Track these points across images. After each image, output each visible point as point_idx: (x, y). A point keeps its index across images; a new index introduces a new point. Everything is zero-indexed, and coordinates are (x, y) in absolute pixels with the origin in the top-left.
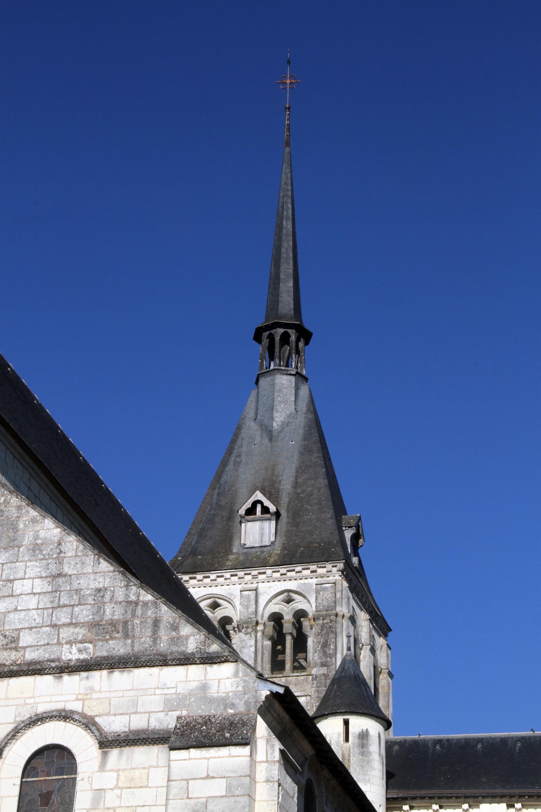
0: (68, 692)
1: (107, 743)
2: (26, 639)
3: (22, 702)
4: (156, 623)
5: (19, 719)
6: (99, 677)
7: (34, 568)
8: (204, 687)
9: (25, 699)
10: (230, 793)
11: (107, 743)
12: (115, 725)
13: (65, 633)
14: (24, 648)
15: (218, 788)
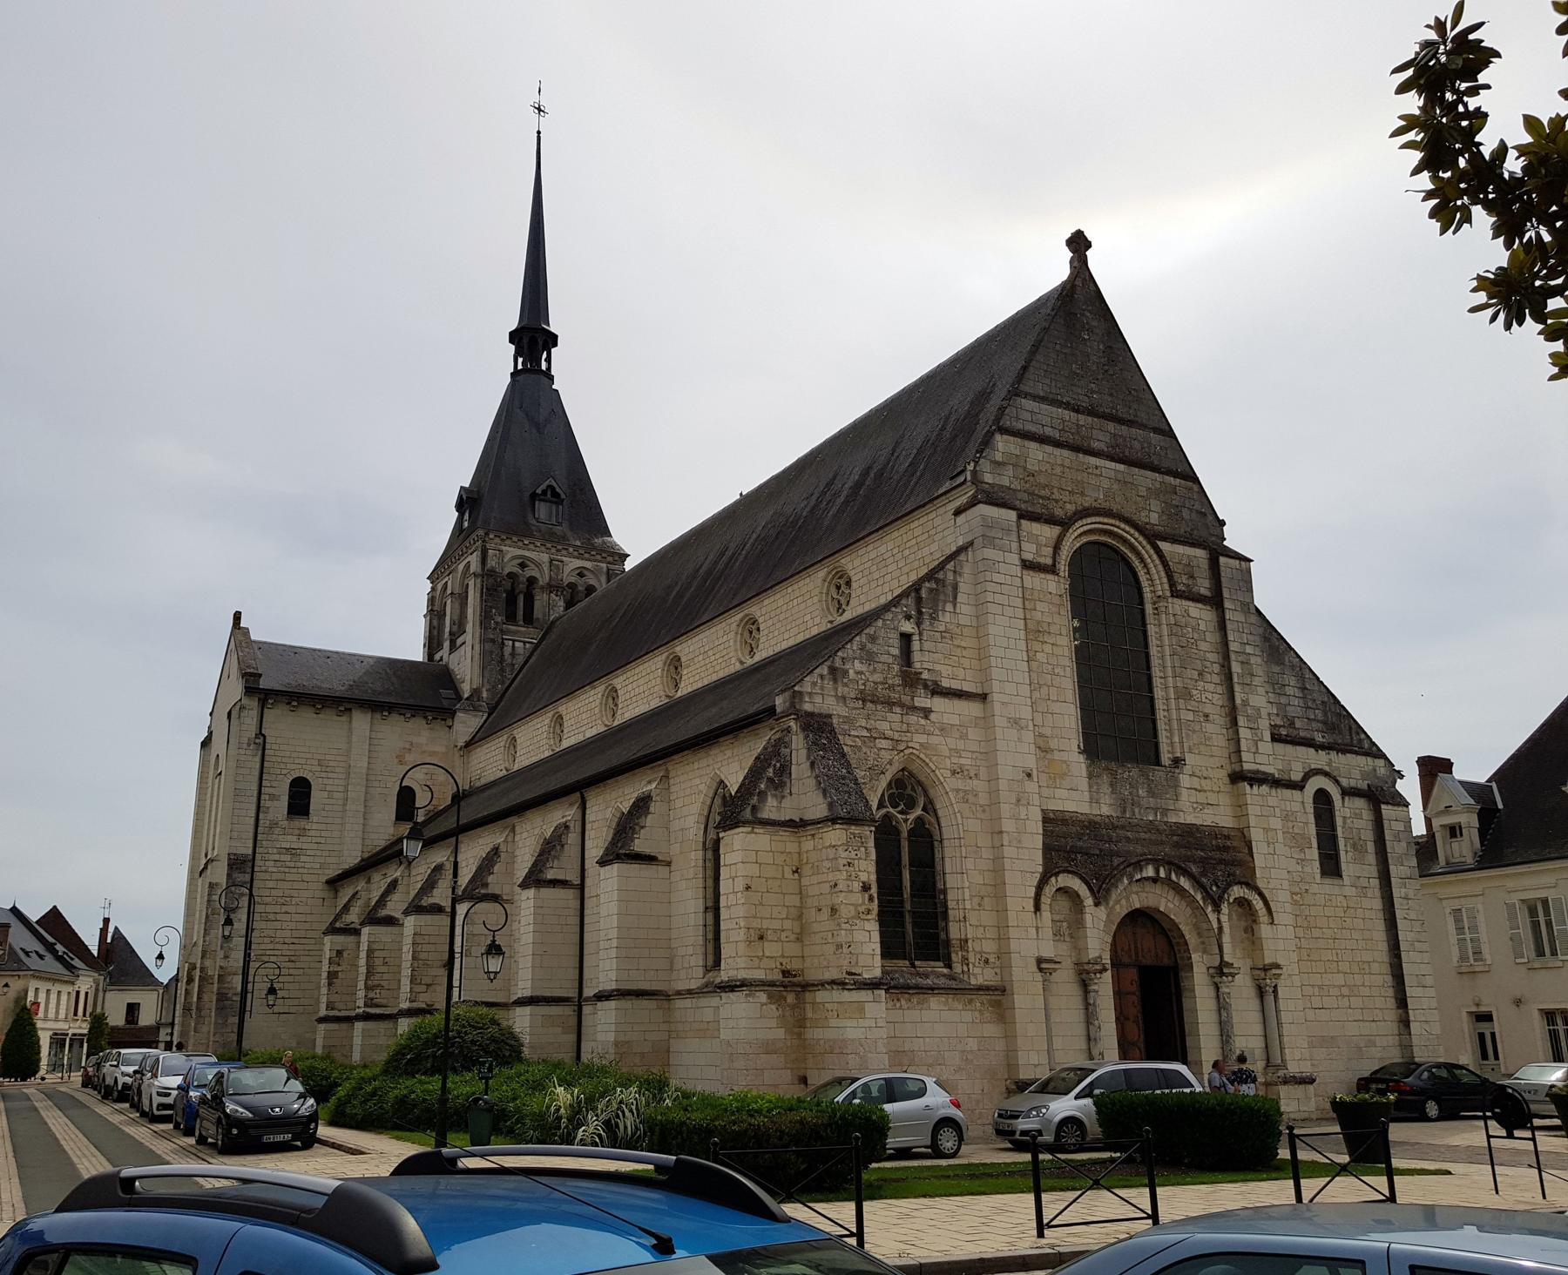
2: (1298, 724)
13: (1314, 725)
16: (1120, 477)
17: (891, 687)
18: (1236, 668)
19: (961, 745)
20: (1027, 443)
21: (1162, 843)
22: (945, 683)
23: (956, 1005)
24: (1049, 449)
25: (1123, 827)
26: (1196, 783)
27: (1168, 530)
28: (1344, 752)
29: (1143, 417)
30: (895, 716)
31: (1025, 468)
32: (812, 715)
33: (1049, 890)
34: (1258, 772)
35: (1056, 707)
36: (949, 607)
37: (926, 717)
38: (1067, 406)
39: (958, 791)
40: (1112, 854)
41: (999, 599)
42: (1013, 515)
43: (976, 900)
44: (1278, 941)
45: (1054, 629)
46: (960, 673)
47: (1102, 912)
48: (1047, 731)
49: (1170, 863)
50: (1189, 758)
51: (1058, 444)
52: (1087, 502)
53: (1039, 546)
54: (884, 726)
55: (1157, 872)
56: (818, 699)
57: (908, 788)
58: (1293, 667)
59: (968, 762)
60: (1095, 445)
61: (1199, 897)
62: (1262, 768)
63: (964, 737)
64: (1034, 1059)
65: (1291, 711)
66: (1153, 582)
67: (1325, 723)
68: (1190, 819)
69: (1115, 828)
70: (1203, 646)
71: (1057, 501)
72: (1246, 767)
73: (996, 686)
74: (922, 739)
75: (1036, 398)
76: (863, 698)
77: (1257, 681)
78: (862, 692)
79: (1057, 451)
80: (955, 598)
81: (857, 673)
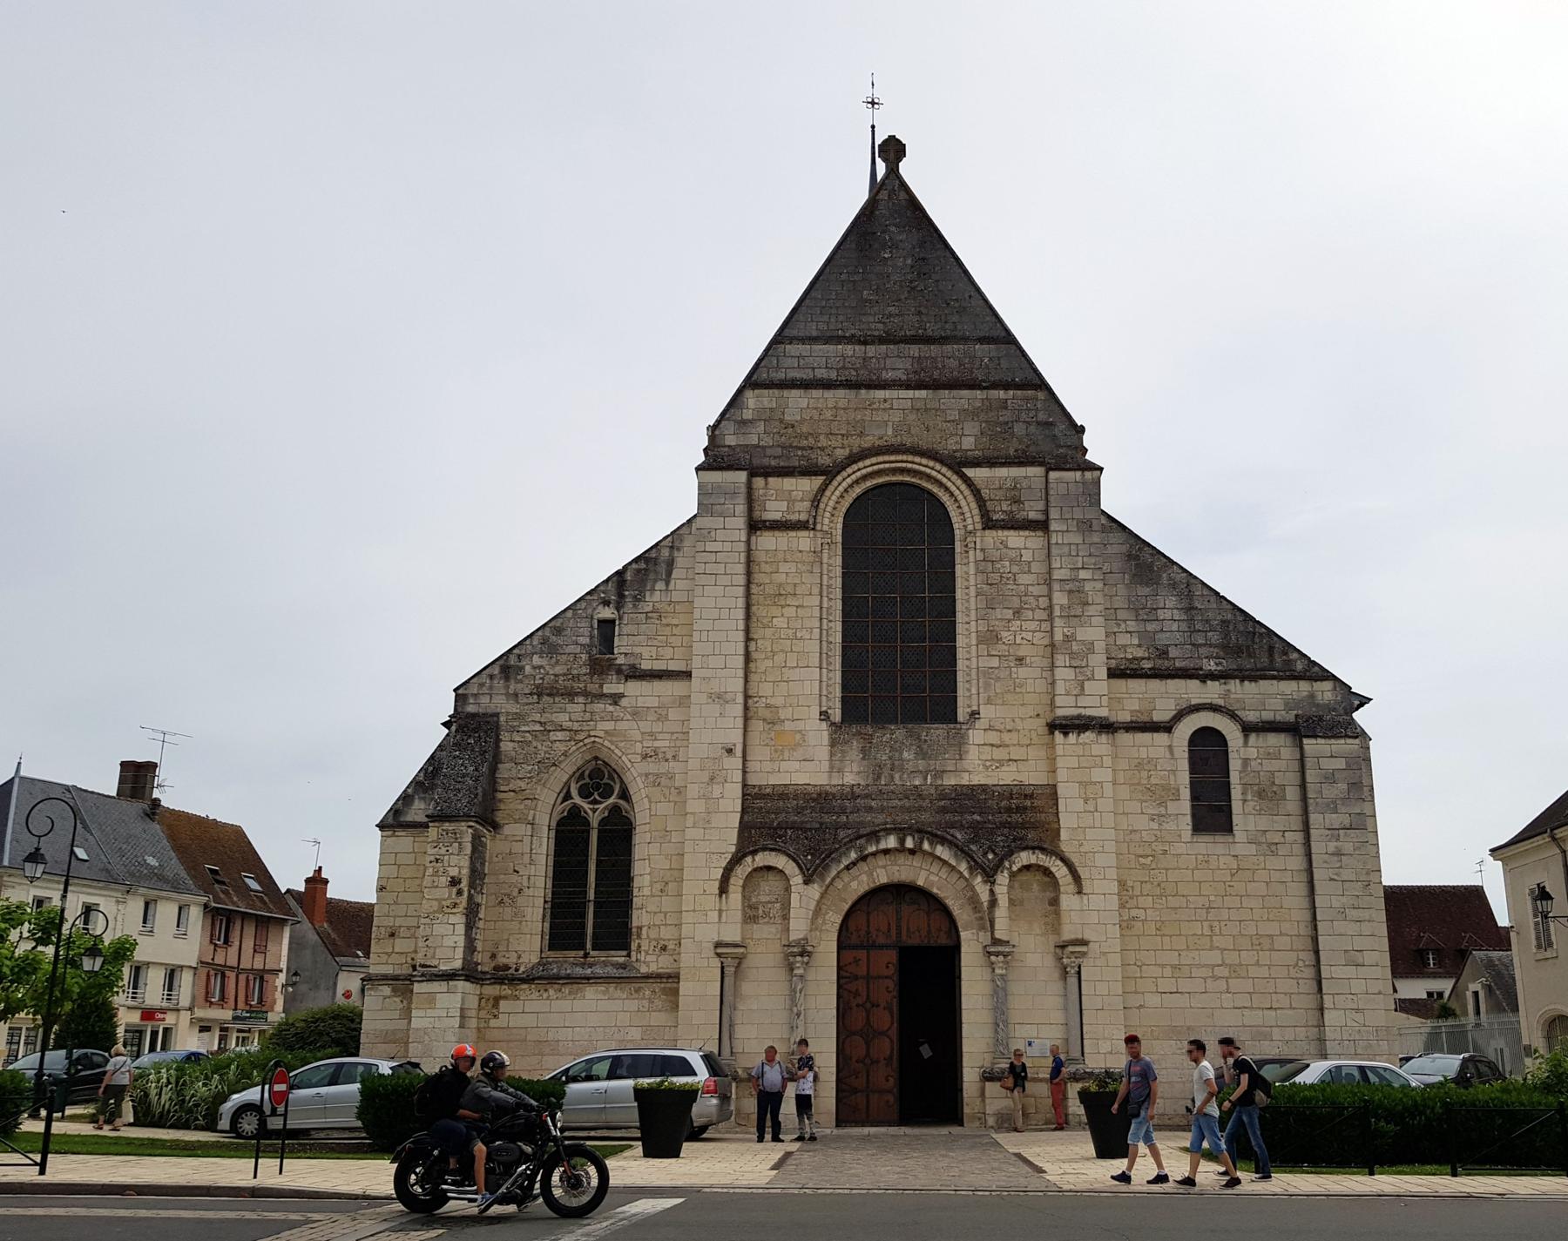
0: (1212, 692)
1: (1248, 729)
2: (1173, 652)
4: (1271, 649)
6: (1234, 685)
7: (1171, 601)
8: (1312, 696)
10: (1349, 768)
11: (1248, 729)
12: (1251, 716)
13: (1203, 651)
15: (1340, 764)
16: (919, 405)
17: (576, 678)
18: (1060, 599)
19: (657, 727)
20: (786, 393)
21: (920, 809)
22: (646, 665)
23: (618, 993)
24: (816, 393)
25: (867, 796)
26: (993, 737)
27: (987, 453)
28: (1254, 679)
30: (576, 708)
31: (781, 421)
32: (474, 715)
33: (741, 872)
34: (1079, 717)
35: (794, 674)
36: (660, 585)
37: (616, 703)
38: (851, 340)
39: (647, 775)
40: (837, 827)
41: (710, 568)
42: (742, 476)
43: (658, 886)
44: (1090, 912)
46: (668, 652)
47: (815, 891)
48: (779, 701)
49: (919, 831)
50: (986, 712)
51: (827, 385)
52: (867, 442)
53: (791, 501)
54: (563, 718)
55: (902, 841)
56: (485, 700)
57: (599, 778)
58: (1174, 585)
59: (667, 744)
60: (889, 375)
61: (963, 867)
62: (1089, 712)
63: (662, 718)
65: (1163, 639)
66: (963, 514)
67: (1224, 647)
68: (978, 779)
69: (855, 797)
70: (1024, 579)
71: (823, 449)
72: (1060, 712)
73: (696, 663)
74: (609, 726)
75: (802, 340)
76: (539, 692)
77: (1091, 610)
78: (537, 687)
79: (829, 394)
80: (669, 574)
81: (534, 668)
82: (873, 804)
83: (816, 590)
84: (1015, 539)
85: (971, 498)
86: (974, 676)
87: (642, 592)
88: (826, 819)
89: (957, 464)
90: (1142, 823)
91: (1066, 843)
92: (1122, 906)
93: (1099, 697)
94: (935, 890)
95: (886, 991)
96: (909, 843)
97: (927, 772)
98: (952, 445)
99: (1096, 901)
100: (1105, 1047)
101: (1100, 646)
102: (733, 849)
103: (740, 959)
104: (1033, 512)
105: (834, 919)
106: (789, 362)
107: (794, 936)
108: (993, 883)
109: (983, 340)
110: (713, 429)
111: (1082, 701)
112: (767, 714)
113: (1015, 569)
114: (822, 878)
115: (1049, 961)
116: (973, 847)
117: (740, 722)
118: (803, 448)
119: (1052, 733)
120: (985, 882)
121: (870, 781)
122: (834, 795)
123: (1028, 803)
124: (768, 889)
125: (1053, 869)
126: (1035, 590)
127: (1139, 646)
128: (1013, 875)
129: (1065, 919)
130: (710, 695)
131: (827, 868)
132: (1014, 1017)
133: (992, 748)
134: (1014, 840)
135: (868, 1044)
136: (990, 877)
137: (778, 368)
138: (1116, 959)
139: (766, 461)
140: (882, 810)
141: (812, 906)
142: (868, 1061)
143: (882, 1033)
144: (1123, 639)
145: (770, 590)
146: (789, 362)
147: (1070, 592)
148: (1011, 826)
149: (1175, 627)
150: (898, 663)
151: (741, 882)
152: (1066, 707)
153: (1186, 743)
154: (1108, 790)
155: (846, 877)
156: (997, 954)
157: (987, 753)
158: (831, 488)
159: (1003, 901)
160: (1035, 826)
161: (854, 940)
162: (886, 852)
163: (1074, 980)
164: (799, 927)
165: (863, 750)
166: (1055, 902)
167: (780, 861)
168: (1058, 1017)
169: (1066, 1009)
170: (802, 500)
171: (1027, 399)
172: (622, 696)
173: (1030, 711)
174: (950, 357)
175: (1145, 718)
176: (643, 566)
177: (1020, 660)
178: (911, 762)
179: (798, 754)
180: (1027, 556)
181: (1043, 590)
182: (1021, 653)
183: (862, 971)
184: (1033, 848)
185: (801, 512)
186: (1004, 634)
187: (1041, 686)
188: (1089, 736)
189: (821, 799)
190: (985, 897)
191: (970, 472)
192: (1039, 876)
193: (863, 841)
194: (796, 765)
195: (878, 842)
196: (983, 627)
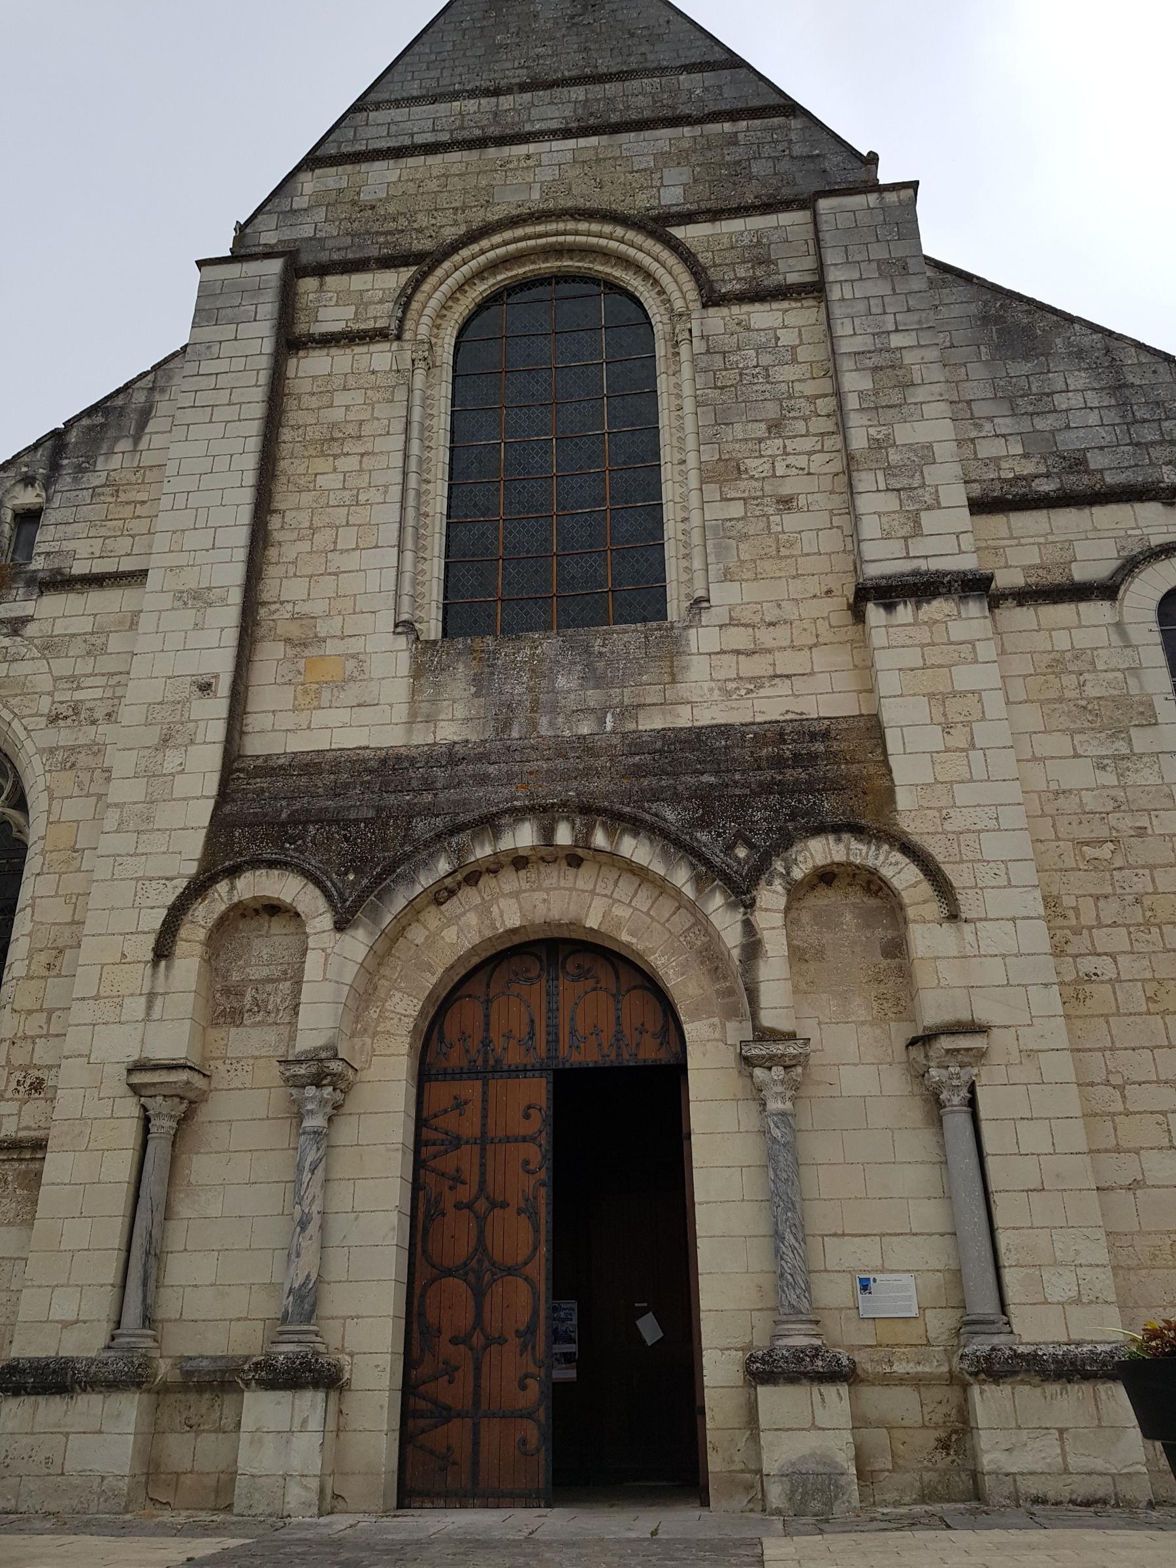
2: (1096, 461)
3: (1122, 533)
5: (1124, 554)
7: (1078, 380)
9: (1126, 530)
14: (1101, 471)
16: (585, 156)
18: (855, 382)
19: (84, 667)
20: (364, 167)
21: (587, 773)
22: (79, 568)
26: (739, 638)
29: (663, 56)
31: (354, 203)
33: (205, 913)
34: (916, 573)
35: (350, 562)
36: (124, 445)
37: (15, 633)
39: (52, 751)
40: (411, 813)
43: (43, 958)
45: (367, 430)
47: (357, 944)
48: (317, 607)
50: (721, 595)
55: (548, 833)
58: (1080, 354)
59: (98, 693)
61: (681, 877)
62: (935, 565)
64: (64, 1308)
65: (1070, 442)
71: (420, 231)
72: (872, 571)
77: (920, 394)
82: (491, 769)
83: (398, 426)
84: (762, 316)
85: (679, 268)
86: (696, 538)
87: (91, 458)
88: (391, 800)
89: (657, 225)
90: (1078, 775)
91: (910, 811)
92: (1058, 952)
93: (950, 540)
94: (625, 937)
95: (523, 1171)
96: (564, 836)
97: (604, 710)
98: (642, 201)
99: (994, 937)
100: (1060, 1286)
101: (945, 450)
102: (192, 868)
103: (189, 1107)
104: (795, 271)
105: (403, 1009)
106: (372, 132)
107: (306, 1042)
108: (750, 906)
109: (689, 68)
110: (241, 229)
111: (918, 547)
112: (294, 631)
113: (766, 360)
114: (375, 914)
115: (896, 1082)
116: (703, 836)
117: (231, 637)
118: (386, 233)
119: (858, 614)
120: (732, 906)
121: (489, 734)
122: (412, 761)
123: (819, 747)
124: (265, 948)
125: (887, 872)
126: (809, 388)
127: (1026, 456)
128: (796, 892)
129: (923, 976)
130: (179, 595)
131: (385, 895)
132: (821, 1217)
133: (740, 650)
134: (793, 817)
135: (479, 1294)
136: (742, 893)
137: (355, 139)
138: (1062, 1067)
139: (324, 257)
140: (510, 778)
141: (350, 973)
142: (477, 1339)
143: (512, 1271)
144: (987, 449)
145: (314, 433)
146: (372, 132)
147: (876, 369)
148: (783, 789)
149: (1093, 418)
150: (551, 523)
151: (202, 934)
152: (885, 560)
153: (1153, 616)
154: (995, 704)
155: (432, 917)
156: (768, 1062)
157: (728, 667)
158: (432, 280)
159: (775, 943)
160: (835, 786)
161: (456, 1059)
162: (520, 862)
163: (958, 1122)
164: (316, 1024)
165: (477, 680)
166: (897, 948)
167: (285, 887)
168: (928, 1214)
169: (948, 1196)
170: (381, 302)
171: (773, 129)
172: (26, 620)
173: (813, 586)
174: (638, 96)
175: (1057, 578)
176: (99, 419)
177: (786, 503)
178: (572, 695)
179: (352, 693)
180: (788, 338)
181: (826, 386)
182: (786, 490)
183: (470, 1126)
184: (837, 830)
185: (381, 315)
186: (751, 463)
187: (831, 541)
188: (938, 608)
189: (388, 768)
190: (732, 936)
191: (678, 232)
192: (857, 897)
193: (463, 837)
194: (343, 715)
195: (497, 835)
196: (709, 454)
